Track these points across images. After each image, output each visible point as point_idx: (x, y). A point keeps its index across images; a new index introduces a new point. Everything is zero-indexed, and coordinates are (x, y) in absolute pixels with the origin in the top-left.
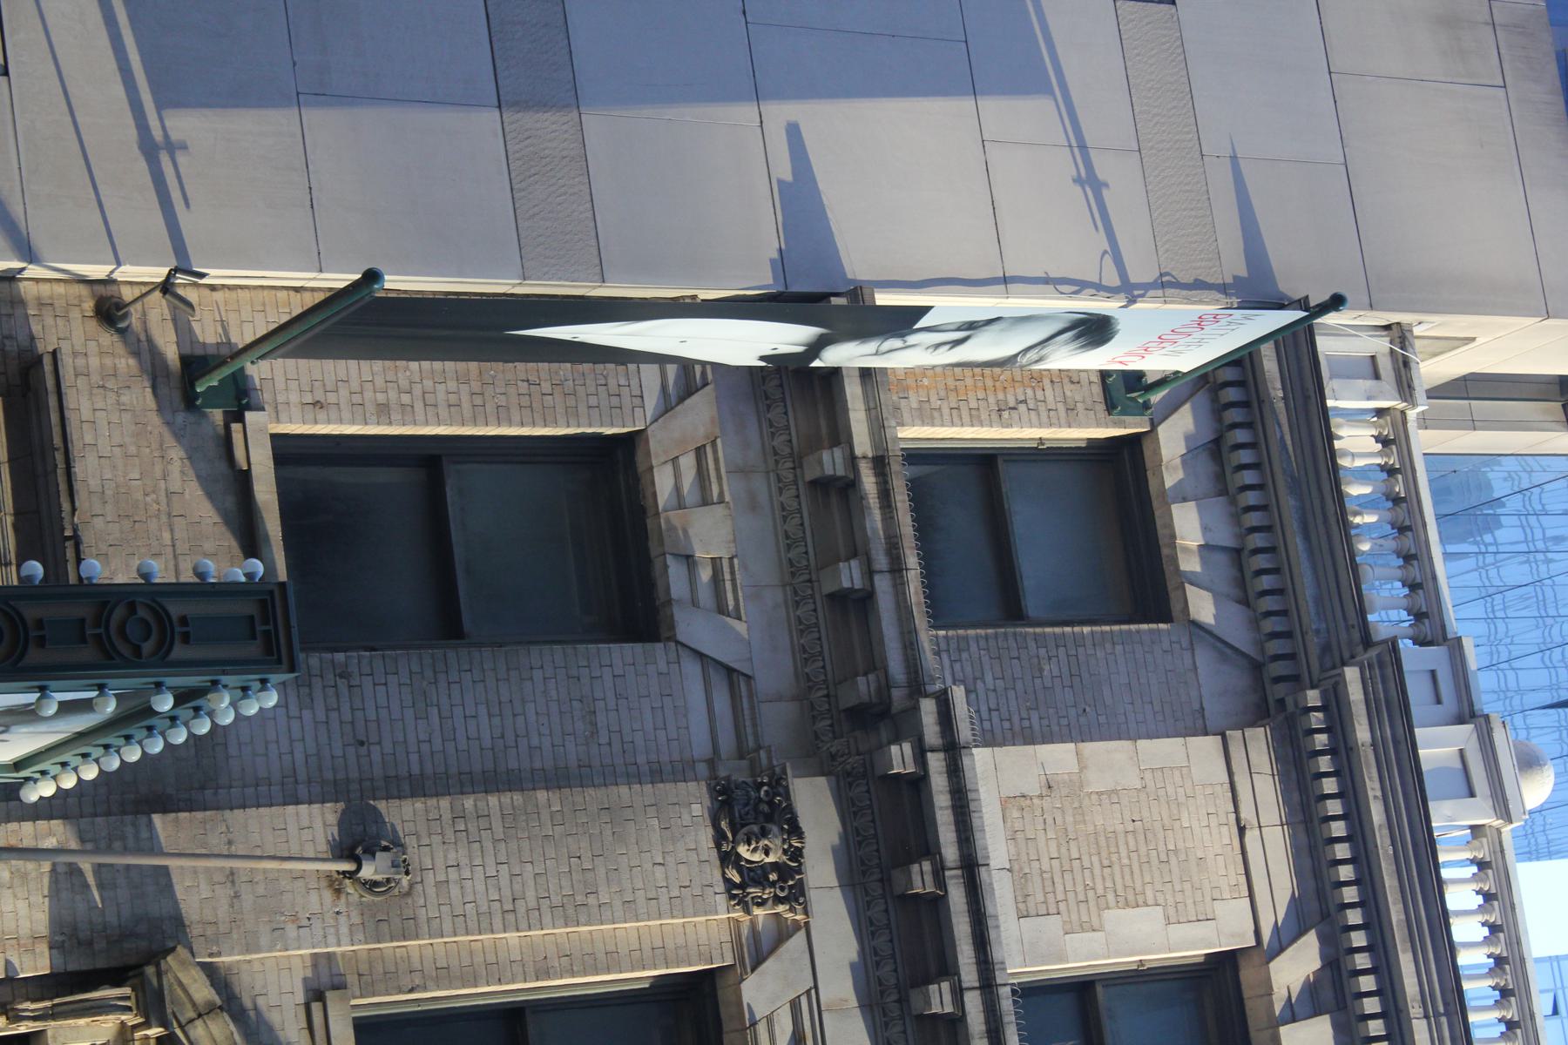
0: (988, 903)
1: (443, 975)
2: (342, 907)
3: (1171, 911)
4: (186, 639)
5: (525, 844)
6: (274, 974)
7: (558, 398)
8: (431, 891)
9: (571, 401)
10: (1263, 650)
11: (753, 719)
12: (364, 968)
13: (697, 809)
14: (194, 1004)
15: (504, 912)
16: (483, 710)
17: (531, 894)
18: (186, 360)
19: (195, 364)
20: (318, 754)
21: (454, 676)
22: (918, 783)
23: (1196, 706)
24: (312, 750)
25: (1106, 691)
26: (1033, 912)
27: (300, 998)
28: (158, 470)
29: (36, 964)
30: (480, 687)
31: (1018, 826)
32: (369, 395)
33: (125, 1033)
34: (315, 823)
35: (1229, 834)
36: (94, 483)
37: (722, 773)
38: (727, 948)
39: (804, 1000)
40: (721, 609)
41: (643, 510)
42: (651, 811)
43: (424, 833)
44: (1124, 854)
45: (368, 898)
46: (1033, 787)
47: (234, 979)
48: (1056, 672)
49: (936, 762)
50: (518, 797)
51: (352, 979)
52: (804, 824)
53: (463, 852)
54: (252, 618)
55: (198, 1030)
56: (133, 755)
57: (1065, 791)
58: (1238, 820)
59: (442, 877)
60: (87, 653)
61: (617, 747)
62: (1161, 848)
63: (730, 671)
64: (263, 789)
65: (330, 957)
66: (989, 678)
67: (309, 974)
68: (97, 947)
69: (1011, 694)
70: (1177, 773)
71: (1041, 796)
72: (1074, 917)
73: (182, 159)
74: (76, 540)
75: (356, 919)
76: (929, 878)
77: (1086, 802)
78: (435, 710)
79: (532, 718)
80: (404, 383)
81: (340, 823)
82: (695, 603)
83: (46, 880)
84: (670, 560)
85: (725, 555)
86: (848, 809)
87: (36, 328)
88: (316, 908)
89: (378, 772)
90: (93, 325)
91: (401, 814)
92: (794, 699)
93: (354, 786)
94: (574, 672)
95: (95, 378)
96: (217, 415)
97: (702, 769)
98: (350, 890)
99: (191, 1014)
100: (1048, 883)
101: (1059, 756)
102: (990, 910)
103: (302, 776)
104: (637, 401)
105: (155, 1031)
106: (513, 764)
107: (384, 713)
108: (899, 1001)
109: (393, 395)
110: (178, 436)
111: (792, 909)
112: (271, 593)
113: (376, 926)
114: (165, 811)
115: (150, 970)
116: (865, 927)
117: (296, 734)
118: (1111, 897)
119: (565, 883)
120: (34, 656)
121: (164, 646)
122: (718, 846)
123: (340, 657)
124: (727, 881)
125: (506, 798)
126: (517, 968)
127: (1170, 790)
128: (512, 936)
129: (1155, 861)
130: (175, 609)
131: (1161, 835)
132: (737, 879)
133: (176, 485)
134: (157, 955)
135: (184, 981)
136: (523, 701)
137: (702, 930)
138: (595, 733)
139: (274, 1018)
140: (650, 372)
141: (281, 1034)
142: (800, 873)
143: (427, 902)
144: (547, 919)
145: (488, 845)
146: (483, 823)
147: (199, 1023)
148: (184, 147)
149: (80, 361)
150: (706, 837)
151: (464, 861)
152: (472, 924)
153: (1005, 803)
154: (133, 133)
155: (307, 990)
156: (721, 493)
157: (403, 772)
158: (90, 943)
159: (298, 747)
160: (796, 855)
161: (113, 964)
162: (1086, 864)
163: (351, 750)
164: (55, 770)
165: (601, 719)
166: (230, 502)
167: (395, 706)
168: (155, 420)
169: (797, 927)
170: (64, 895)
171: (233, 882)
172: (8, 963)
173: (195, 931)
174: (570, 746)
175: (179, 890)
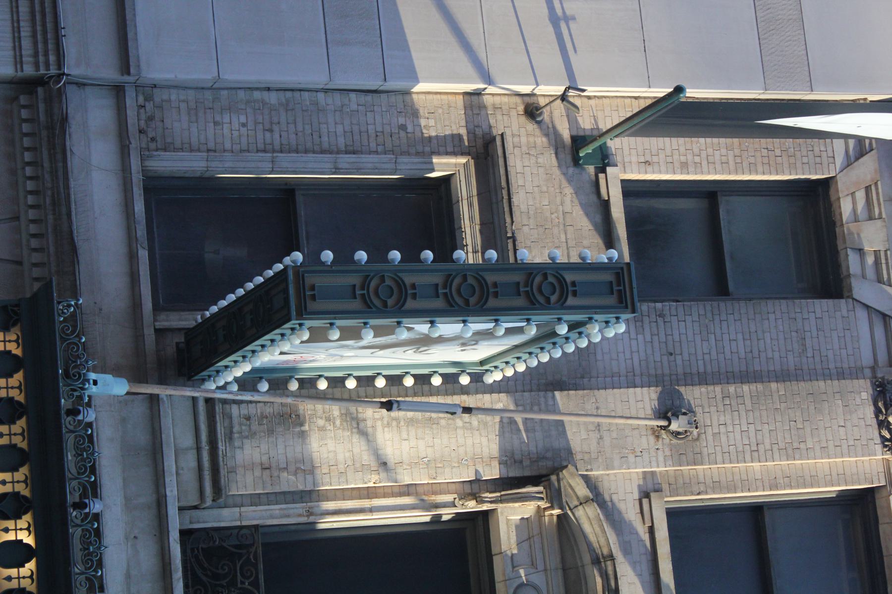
1: (717, 486)
2: (660, 445)
4: (575, 294)
5: (764, 413)
6: (622, 482)
7: (785, 158)
8: (710, 438)
9: (792, 160)
12: (672, 480)
13: (864, 395)
14: (578, 498)
15: (752, 451)
16: (740, 336)
17: (767, 442)
18: (574, 139)
19: (579, 141)
20: (646, 360)
21: (724, 317)
24: (643, 357)
28: (558, 199)
29: (492, 472)
30: (738, 323)
32: (676, 157)
33: (540, 511)
34: (646, 398)
36: (523, 208)
37: (879, 375)
38: (882, 475)
40: (880, 280)
41: (834, 224)
42: (838, 396)
43: (706, 406)
45: (675, 441)
47: (600, 484)
50: (760, 386)
51: (665, 487)
53: (728, 417)
54: (611, 282)
55: (580, 512)
56: (545, 358)
59: (716, 431)
60: (520, 301)
61: (817, 359)
63: (884, 316)
64: (615, 379)
65: (653, 473)
67: (641, 482)
68: (524, 464)
73: (572, 25)
74: (514, 238)
75: (668, 453)
78: (713, 336)
79: (768, 341)
80: (696, 151)
81: (659, 399)
82: (864, 276)
83: (497, 426)
84: (849, 251)
85: (882, 249)
87: (492, 122)
88: (645, 446)
89: (680, 370)
90: (523, 119)
91: (693, 394)
93: (667, 378)
94: (793, 315)
95: (524, 149)
96: (591, 169)
97: (868, 372)
98: (665, 437)
99: (576, 503)
103: (637, 372)
104: (831, 160)
105: (557, 511)
106: (757, 368)
107: (683, 337)
109: (690, 157)
110: (569, 181)
112: (622, 269)
113: (679, 457)
114: (561, 390)
115: (553, 478)
117: (634, 349)
119: (787, 436)
120: (492, 303)
121: (563, 298)
122: (877, 417)
123: (659, 305)
124: (882, 437)
125: (753, 387)
126: (759, 483)
128: (756, 465)
130: (569, 277)
132: (888, 436)
133: (568, 207)
134: (557, 469)
135: (573, 484)
136: (764, 332)
137: (867, 465)
138: (805, 350)
139: (622, 506)
140: (839, 144)
141: (625, 516)
143: (708, 445)
144: (776, 455)
145: (743, 413)
146: (740, 401)
147: (580, 508)
148: (573, 18)
149: (516, 140)
150: (870, 411)
151: (729, 422)
152: (734, 457)
154: (545, 11)
155: (640, 492)
156: (880, 213)
157: (694, 370)
158: (521, 462)
159: (635, 356)
161: (534, 473)
163: (665, 358)
164: (503, 366)
165: (808, 342)
166: (598, 218)
167: (690, 333)
168: (556, 172)
170: (507, 435)
171: (599, 430)
172: (477, 472)
173: (578, 457)
174: (790, 358)
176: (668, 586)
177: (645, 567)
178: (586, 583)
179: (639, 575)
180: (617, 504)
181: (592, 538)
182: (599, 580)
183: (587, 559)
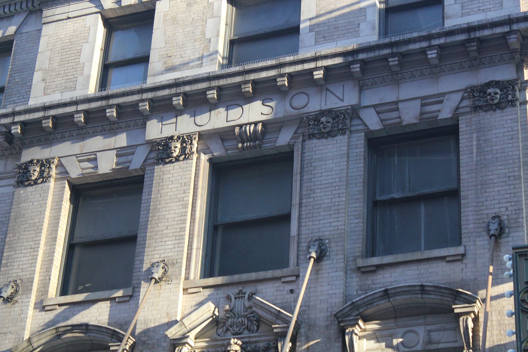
0: (54, 103)
3: (85, 41)
5: (18, 245)
8: (23, 273)
10: (26, 11)
11: (9, 173)
12: (41, 294)
13: (22, 192)
14: (28, 346)
22: (23, 124)
23: (37, 32)
25: (27, 61)
26: (75, 86)
27: (44, 313)
31: (51, 90)
35: (69, 22)
39: (79, 159)
44: (66, 56)
45: (20, 292)
46: (43, 85)
48: (18, 77)
49: (17, 119)
50: (6, 247)
51: (43, 297)
52: (30, 160)
57: (46, 75)
58: (66, 19)
62: (68, 44)
66: (15, 99)
67: (38, 310)
69: (21, 91)
70: (50, 39)
71: (46, 83)
72: (79, 72)
75: (25, 296)
76: (47, 121)
77: (50, 68)
86: (31, 145)
88: (19, 308)
92: (7, 160)
98: (17, 298)
99: (31, 346)
100: (69, 80)
101: (37, 77)
102: (56, 102)
108: (82, 129)
111: (53, 163)
116: (63, 139)
118: (77, 60)
119: (30, 232)
122: (32, 185)
125: (5, 250)
127: (54, 41)
129: (71, 46)
131: (64, 44)
132: (41, 179)
139: (47, 320)
141: (51, 319)
142: (42, 160)
143: (24, 275)
146: (10, 257)
147: (33, 345)
150: (29, 189)
151: (18, 263)
153: (45, 94)
160: (38, 161)
162: (66, 68)
169: (59, 161)
175: (4, 349)
176: (86, 297)
177: (76, 308)
178: (74, 341)
179: (79, 312)
180: (45, 323)
181: (48, 338)
182: (68, 335)
183: (59, 341)
